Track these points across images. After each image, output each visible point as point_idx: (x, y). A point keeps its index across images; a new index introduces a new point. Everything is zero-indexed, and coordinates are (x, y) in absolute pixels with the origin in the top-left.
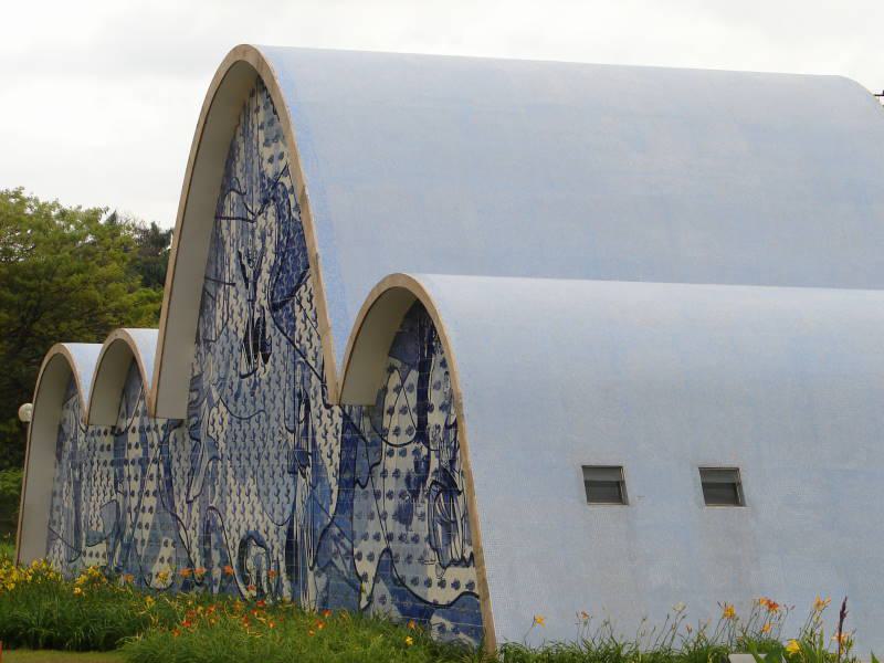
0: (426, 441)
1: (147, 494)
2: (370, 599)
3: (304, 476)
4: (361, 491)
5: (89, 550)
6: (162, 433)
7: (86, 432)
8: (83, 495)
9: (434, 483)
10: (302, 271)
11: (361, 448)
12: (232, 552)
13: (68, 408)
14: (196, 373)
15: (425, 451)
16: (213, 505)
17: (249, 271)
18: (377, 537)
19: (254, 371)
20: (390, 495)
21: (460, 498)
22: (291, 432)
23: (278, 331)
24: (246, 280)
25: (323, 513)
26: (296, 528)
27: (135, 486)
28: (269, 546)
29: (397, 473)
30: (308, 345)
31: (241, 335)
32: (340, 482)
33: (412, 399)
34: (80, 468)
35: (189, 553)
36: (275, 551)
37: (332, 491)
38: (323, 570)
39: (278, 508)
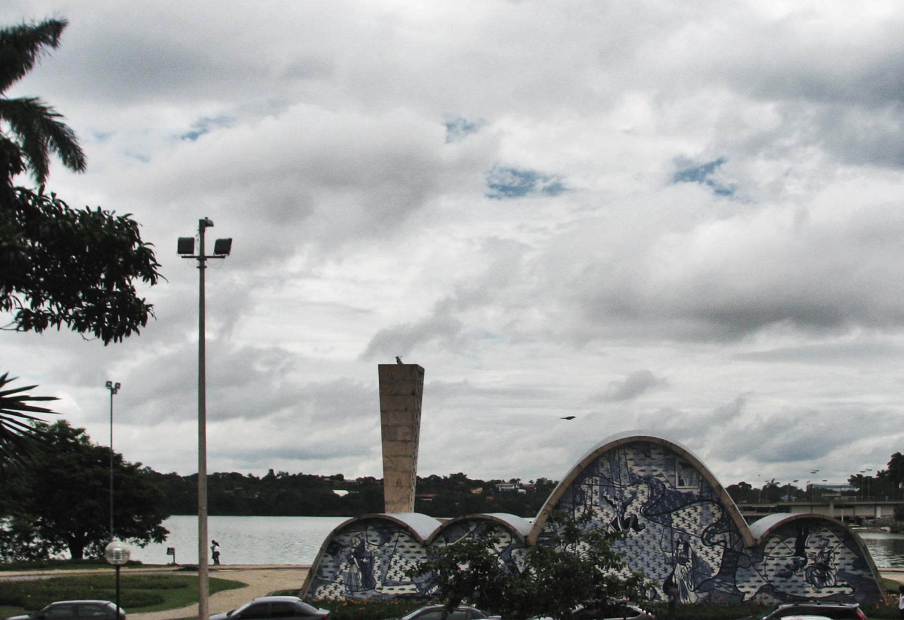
0: (805, 556)
2: (752, 599)
3: (685, 565)
4: (744, 569)
5: (384, 587)
6: (500, 550)
7: (379, 546)
8: (375, 568)
9: (809, 567)
10: (679, 506)
13: (348, 536)
14: (546, 531)
15: (802, 559)
17: (615, 502)
18: (760, 581)
20: (772, 570)
22: (670, 552)
23: (651, 522)
24: (614, 506)
25: (703, 576)
29: (777, 565)
30: (686, 528)
31: (607, 521)
32: (721, 568)
33: (793, 545)
38: (705, 591)
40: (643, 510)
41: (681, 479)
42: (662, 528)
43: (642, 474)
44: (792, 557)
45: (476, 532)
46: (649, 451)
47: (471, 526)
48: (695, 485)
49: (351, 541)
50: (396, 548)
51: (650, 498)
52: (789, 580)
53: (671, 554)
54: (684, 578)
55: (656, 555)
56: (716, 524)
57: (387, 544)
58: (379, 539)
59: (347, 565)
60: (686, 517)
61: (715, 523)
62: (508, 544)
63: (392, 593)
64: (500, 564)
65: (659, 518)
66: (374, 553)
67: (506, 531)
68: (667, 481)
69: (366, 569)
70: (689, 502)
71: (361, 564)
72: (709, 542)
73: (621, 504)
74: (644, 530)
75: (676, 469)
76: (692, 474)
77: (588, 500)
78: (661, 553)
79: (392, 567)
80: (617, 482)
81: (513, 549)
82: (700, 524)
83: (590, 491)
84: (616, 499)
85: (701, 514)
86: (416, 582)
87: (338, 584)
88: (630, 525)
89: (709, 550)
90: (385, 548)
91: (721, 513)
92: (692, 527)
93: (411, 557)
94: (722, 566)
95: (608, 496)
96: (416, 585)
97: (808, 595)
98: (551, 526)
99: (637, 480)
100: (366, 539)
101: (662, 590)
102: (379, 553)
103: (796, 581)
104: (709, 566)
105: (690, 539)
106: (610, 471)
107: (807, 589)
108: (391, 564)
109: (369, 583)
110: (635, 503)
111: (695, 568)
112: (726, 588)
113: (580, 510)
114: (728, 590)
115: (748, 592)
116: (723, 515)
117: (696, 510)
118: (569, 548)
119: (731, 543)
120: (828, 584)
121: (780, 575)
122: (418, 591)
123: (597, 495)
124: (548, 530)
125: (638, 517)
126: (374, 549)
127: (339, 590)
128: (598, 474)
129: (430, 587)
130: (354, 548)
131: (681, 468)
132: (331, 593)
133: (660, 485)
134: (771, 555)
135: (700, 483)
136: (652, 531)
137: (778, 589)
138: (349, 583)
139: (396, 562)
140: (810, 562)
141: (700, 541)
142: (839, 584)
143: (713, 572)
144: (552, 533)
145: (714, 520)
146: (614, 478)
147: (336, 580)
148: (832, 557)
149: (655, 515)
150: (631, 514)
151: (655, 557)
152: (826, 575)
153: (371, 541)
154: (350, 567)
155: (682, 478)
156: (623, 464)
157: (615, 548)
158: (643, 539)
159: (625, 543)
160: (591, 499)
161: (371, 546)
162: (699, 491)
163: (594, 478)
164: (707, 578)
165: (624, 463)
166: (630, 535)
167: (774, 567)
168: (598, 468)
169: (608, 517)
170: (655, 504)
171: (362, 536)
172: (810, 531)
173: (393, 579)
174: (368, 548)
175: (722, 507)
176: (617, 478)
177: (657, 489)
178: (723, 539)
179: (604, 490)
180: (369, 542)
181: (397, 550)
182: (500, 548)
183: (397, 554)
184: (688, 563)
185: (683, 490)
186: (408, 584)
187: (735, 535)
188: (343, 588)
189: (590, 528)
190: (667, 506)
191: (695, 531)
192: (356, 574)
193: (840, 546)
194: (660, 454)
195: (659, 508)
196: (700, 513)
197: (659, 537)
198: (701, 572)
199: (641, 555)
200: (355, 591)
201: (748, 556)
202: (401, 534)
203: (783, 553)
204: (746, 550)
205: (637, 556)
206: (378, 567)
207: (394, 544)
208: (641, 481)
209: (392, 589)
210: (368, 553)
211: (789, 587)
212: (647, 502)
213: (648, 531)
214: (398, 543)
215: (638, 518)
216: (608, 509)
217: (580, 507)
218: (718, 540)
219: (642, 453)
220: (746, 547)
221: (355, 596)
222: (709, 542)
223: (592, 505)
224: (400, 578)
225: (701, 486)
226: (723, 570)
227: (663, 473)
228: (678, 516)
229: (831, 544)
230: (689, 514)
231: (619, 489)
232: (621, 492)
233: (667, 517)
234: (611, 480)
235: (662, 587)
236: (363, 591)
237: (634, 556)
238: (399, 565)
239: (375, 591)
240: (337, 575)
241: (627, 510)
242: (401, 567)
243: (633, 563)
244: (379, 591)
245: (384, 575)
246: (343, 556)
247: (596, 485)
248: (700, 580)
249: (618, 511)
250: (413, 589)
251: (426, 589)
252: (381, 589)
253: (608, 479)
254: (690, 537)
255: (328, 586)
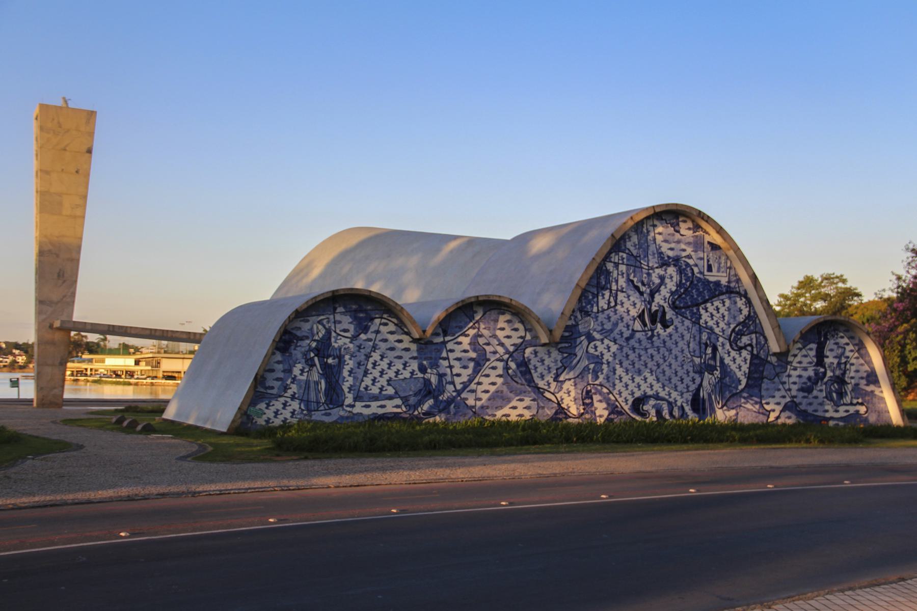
0: (824, 367)
1: (487, 376)
2: (778, 418)
4: (769, 381)
5: (357, 404)
6: (511, 349)
8: (345, 373)
9: (828, 380)
10: (707, 297)
11: (767, 366)
12: (623, 404)
13: (308, 321)
15: (822, 370)
16: (597, 382)
17: (643, 289)
18: (784, 397)
19: (652, 330)
20: (795, 383)
21: (850, 386)
22: (698, 357)
23: (680, 317)
24: (641, 294)
26: (703, 394)
27: (470, 371)
28: (671, 400)
29: (800, 376)
30: (715, 326)
31: (634, 312)
32: (749, 378)
33: (813, 353)
34: (340, 358)
35: (559, 404)
36: (679, 404)
37: (740, 381)
38: (733, 409)
39: (681, 387)
40: (672, 301)
41: (709, 263)
42: (690, 326)
43: (671, 254)
44: (814, 368)
45: (482, 322)
46: (678, 225)
47: (476, 312)
48: (723, 272)
49: (312, 329)
50: (376, 342)
51: (680, 285)
52: (810, 396)
53: (699, 359)
54: (712, 391)
55: (684, 360)
56: (743, 324)
57: (363, 336)
58: (352, 328)
59: (304, 368)
60: (715, 312)
61: (743, 322)
62: (521, 340)
63: (366, 412)
64: (510, 368)
65: (688, 312)
66: (345, 349)
67: (519, 322)
68: (696, 265)
69: (332, 375)
70: (717, 293)
71: (325, 366)
72: (737, 345)
73: (648, 291)
74: (672, 327)
75: (705, 250)
76: (720, 258)
77: (614, 284)
78: (688, 358)
79: (369, 372)
80: (645, 261)
81: (527, 348)
82: (728, 321)
83: (616, 272)
84: (643, 284)
85: (729, 309)
86: (402, 395)
87: (289, 400)
88: (658, 320)
89: (737, 356)
90: (361, 342)
91: (748, 309)
92: (720, 325)
93: (396, 357)
94: (749, 377)
95: (635, 280)
96: (402, 400)
97: (828, 415)
98: (572, 318)
99: (666, 260)
100: (333, 328)
101: (689, 407)
102: (352, 350)
103: (816, 397)
104: (737, 376)
105: (718, 341)
106: (637, 247)
107: (827, 407)
108: (368, 367)
109: (335, 396)
110: (664, 292)
111: (724, 379)
112: (752, 405)
113: (605, 296)
114: (754, 407)
115: (774, 411)
116: (749, 311)
117: (724, 303)
118: (592, 348)
119: (757, 348)
120: (845, 402)
121: (801, 390)
122: (404, 409)
123: (623, 277)
124: (570, 323)
125: (667, 309)
126: (345, 344)
127: (289, 409)
128: (625, 250)
129: (420, 403)
130: (315, 340)
131: (710, 249)
132: (276, 413)
133: (688, 269)
134: (795, 364)
135: (728, 270)
136: (681, 329)
137: (801, 407)
138: (305, 398)
139: (375, 364)
140: (829, 374)
141: (728, 344)
142: (855, 401)
143: (740, 384)
144: (573, 326)
145: (741, 318)
146: (642, 256)
147: (286, 392)
148: (848, 369)
149: (683, 308)
150: (660, 306)
151: (683, 363)
152: (843, 391)
153: (341, 331)
154: (308, 372)
155: (711, 262)
156: (652, 239)
157: (642, 349)
158: (671, 339)
159: (652, 343)
160: (617, 281)
161: (340, 339)
162: (727, 279)
163: (621, 254)
164: (734, 392)
165: (652, 237)
166: (658, 332)
167: (797, 380)
168: (625, 242)
169: (635, 308)
170: (683, 293)
171: (328, 322)
172: (829, 337)
173: (371, 390)
174: (336, 342)
175: (749, 303)
176: (645, 257)
177: (686, 275)
178: (749, 342)
179: (631, 271)
180: (338, 331)
181: (377, 345)
182: (512, 345)
183: (376, 351)
184: (715, 372)
185: (712, 277)
186: (390, 398)
187: (761, 337)
188: (295, 405)
189: (615, 322)
190: (695, 296)
191: (723, 331)
192: (317, 383)
193: (854, 356)
194: (689, 229)
195: (688, 298)
196: (728, 308)
197: (687, 336)
198: (728, 384)
199: (669, 360)
200: (315, 411)
201: (774, 365)
202: (384, 321)
203: (806, 360)
204: (772, 357)
205: (665, 361)
206: (349, 371)
207: (372, 336)
208: (669, 262)
209: (368, 406)
210: (336, 349)
211: (810, 404)
212: (676, 290)
213: (676, 328)
214: (378, 335)
215: (666, 311)
216: (635, 297)
217: (604, 292)
218: (745, 343)
219: (671, 226)
220: (771, 353)
221: (314, 418)
222: (737, 345)
223: (617, 290)
224: (380, 388)
225: (729, 274)
226: (750, 382)
227: (693, 254)
228: (706, 309)
229: (848, 354)
230: (718, 309)
231: (647, 271)
232: (649, 275)
233: (695, 311)
234: (638, 259)
235: (689, 403)
236: (326, 410)
237: (661, 361)
238: (379, 368)
239: (343, 409)
240: (287, 384)
241: (655, 299)
242: (382, 373)
243: (660, 370)
244: (348, 409)
245: (358, 384)
246: (297, 353)
247: (623, 264)
248: (727, 395)
249: (645, 301)
250: (397, 406)
251: (414, 406)
252: (353, 406)
253: (635, 257)
254: (718, 338)
255: (273, 402)
